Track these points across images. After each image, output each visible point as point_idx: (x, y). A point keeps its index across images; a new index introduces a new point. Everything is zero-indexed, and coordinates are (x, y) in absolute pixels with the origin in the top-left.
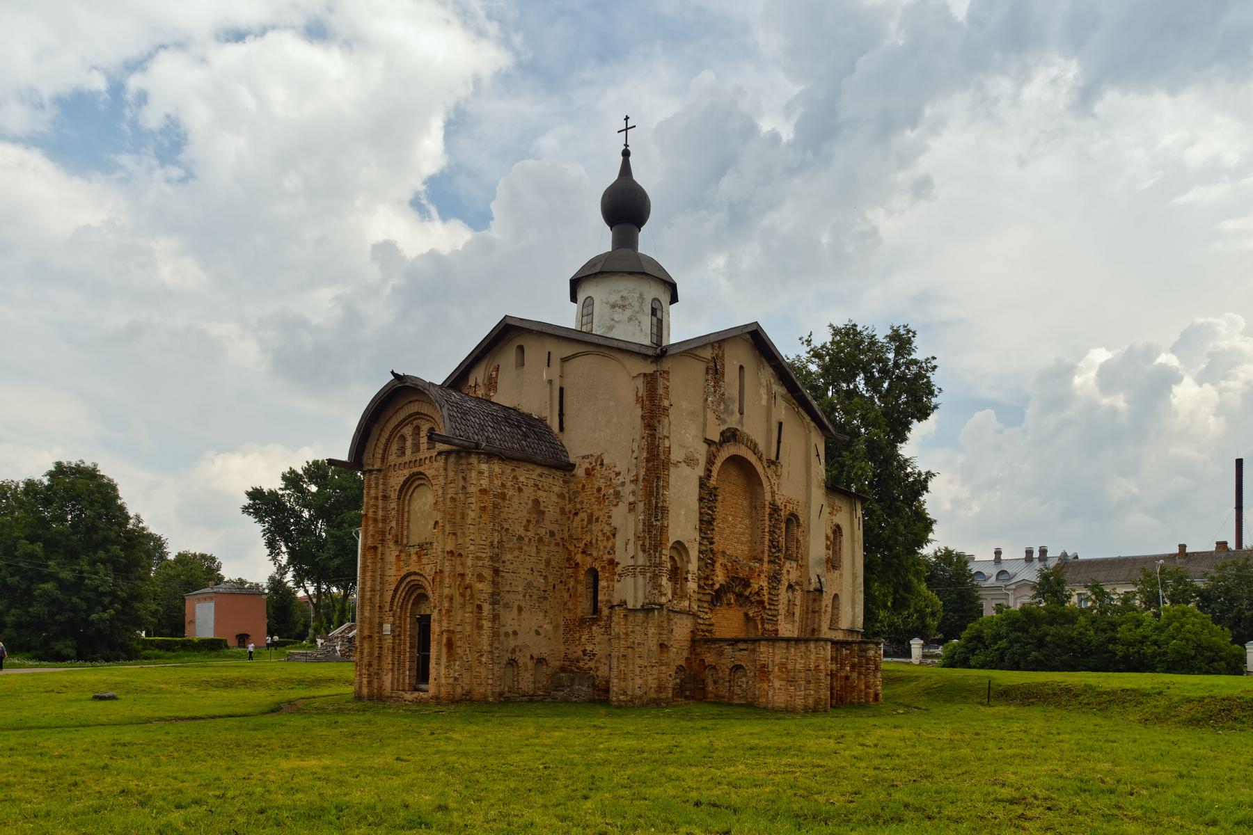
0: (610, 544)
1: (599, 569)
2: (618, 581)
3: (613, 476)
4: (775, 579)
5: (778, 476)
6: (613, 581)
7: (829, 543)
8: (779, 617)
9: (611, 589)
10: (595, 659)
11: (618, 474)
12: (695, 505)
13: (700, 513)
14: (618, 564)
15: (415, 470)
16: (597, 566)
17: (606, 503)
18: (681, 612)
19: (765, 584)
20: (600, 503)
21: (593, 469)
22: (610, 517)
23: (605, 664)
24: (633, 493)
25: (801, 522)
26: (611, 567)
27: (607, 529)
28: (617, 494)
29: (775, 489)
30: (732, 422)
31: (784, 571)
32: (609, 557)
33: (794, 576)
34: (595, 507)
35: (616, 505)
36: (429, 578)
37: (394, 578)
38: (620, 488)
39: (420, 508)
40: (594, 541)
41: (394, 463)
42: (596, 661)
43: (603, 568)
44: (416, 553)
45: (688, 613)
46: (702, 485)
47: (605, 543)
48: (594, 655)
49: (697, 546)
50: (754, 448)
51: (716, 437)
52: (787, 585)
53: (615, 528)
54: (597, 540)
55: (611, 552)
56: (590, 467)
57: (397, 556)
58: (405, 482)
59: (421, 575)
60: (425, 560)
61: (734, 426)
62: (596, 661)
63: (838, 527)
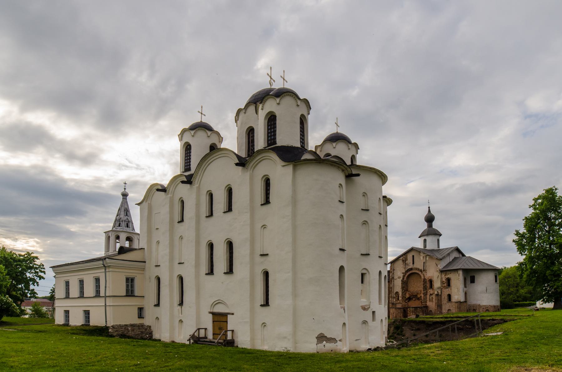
4: (425, 294)
5: (426, 272)
7: (444, 283)
8: (427, 302)
12: (400, 285)
13: (402, 286)
18: (398, 303)
19: (422, 295)
25: (433, 280)
29: (425, 275)
30: (411, 266)
31: (429, 292)
33: (431, 292)
45: (400, 303)
46: (402, 281)
49: (401, 292)
50: (417, 269)
51: (404, 272)
52: (429, 294)
61: (411, 267)
63: (448, 278)
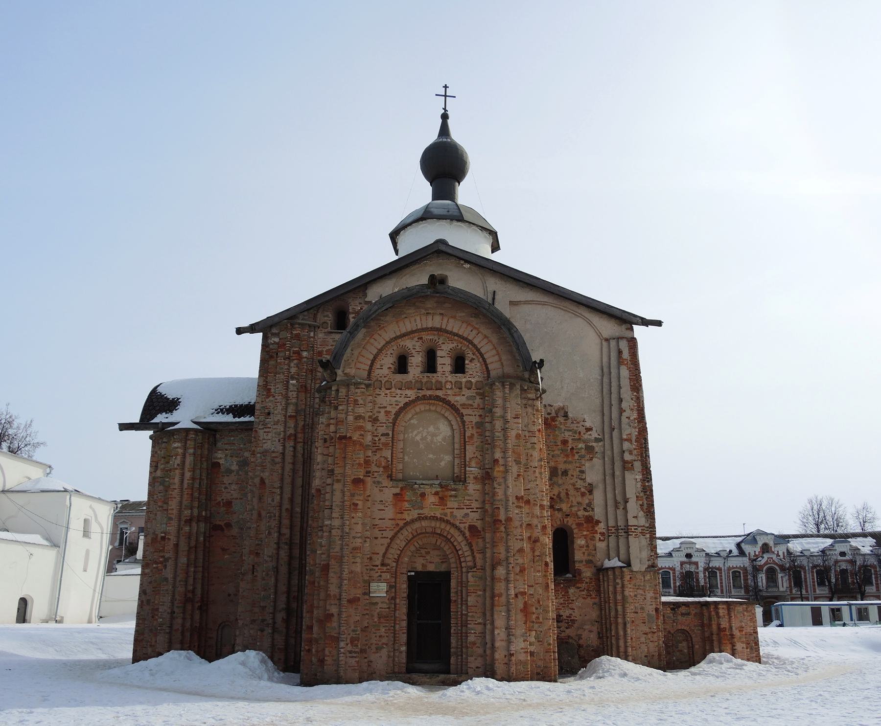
0: (587, 501)
1: (574, 526)
2: (600, 540)
3: (583, 430)
6: (593, 539)
9: (591, 547)
10: (575, 625)
11: (589, 429)
14: (598, 522)
15: (429, 393)
16: (571, 522)
17: (577, 457)
20: (567, 456)
21: (553, 419)
22: (582, 472)
23: (591, 631)
24: (631, 453)
26: (590, 525)
27: (580, 484)
28: (590, 449)
32: (586, 514)
34: (561, 459)
35: (591, 459)
36: (462, 526)
37: (389, 524)
38: (594, 444)
39: (423, 439)
40: (563, 495)
41: (386, 379)
42: (579, 628)
43: (579, 525)
44: (436, 493)
47: (579, 499)
48: (573, 621)
53: (589, 484)
54: (567, 494)
55: (588, 508)
56: (549, 417)
57: (395, 495)
58: (406, 405)
59: (448, 522)
60: (452, 504)
62: (579, 628)
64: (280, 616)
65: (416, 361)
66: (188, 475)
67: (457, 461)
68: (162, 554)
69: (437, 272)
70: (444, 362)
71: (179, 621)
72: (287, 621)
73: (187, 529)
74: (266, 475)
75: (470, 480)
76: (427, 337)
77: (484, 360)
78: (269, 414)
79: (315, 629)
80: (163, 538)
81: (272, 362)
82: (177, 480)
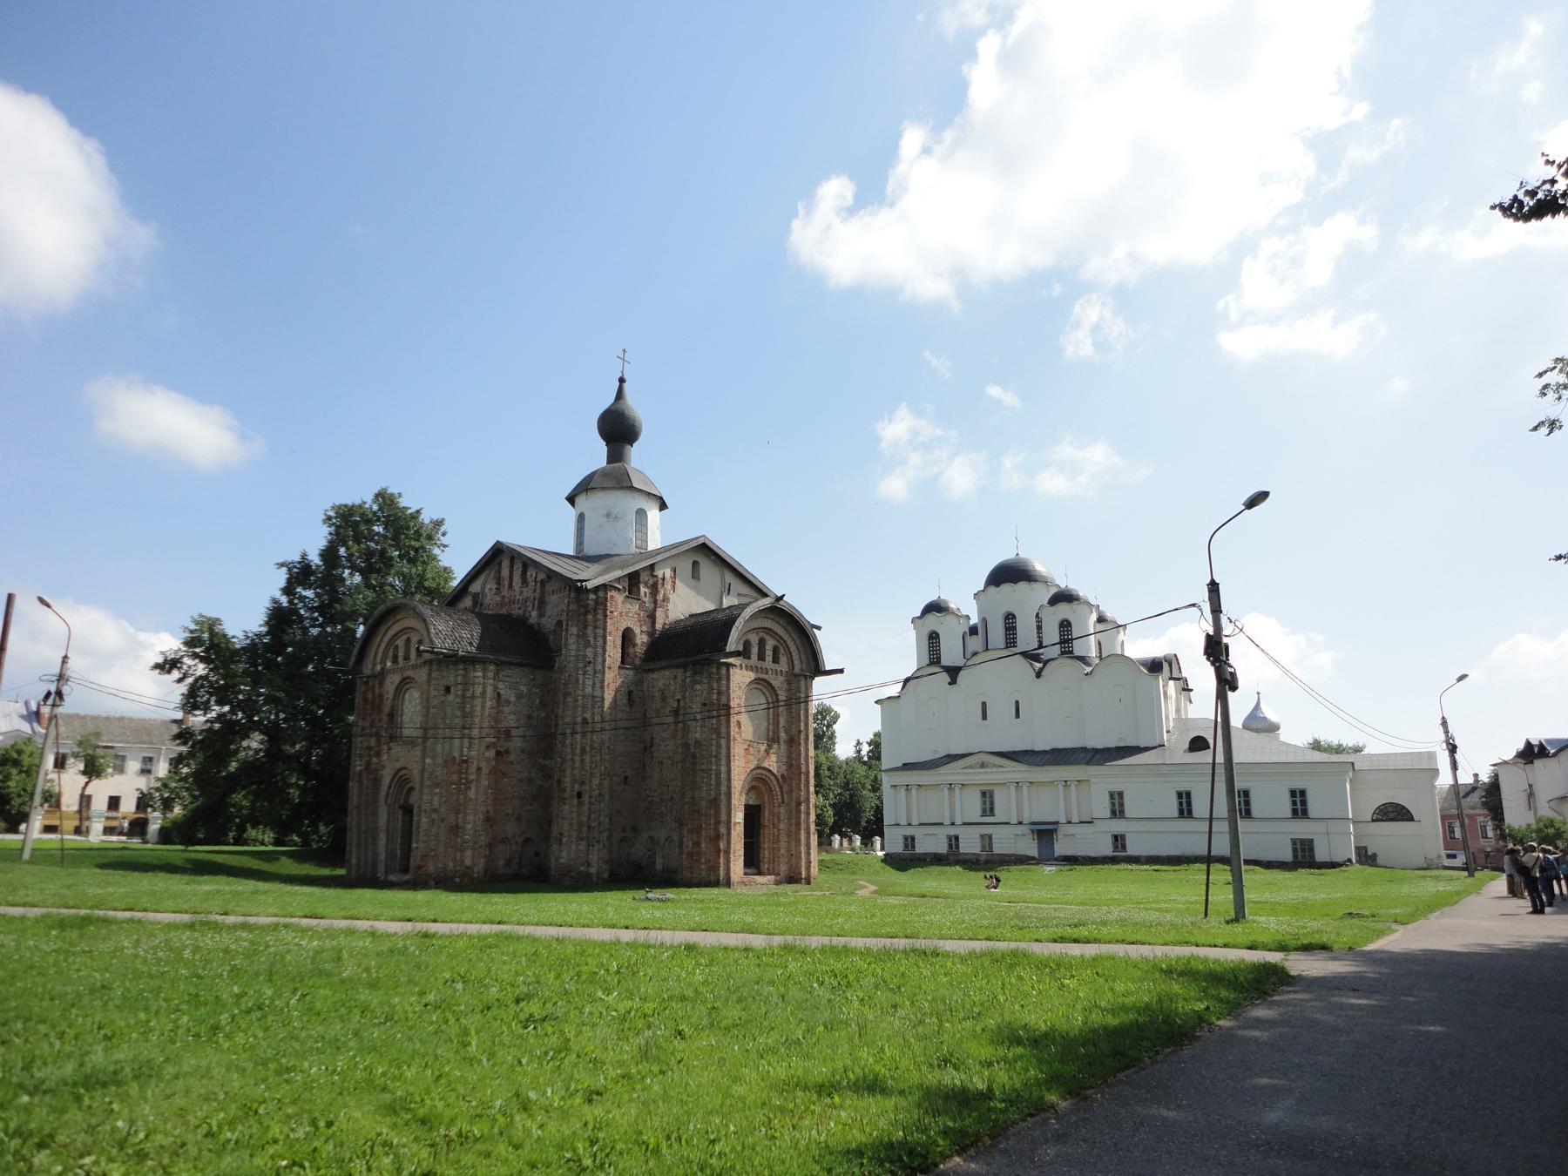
15: (762, 676)
64: (606, 834)
65: (755, 650)
66: (489, 704)
67: (771, 727)
68: (464, 776)
69: (699, 560)
70: (769, 653)
71: (483, 838)
72: (608, 837)
73: (487, 754)
74: (588, 716)
75: (782, 741)
76: (761, 634)
77: (791, 656)
78: (590, 662)
79: (703, 845)
80: (465, 762)
81: (590, 617)
82: (478, 708)
